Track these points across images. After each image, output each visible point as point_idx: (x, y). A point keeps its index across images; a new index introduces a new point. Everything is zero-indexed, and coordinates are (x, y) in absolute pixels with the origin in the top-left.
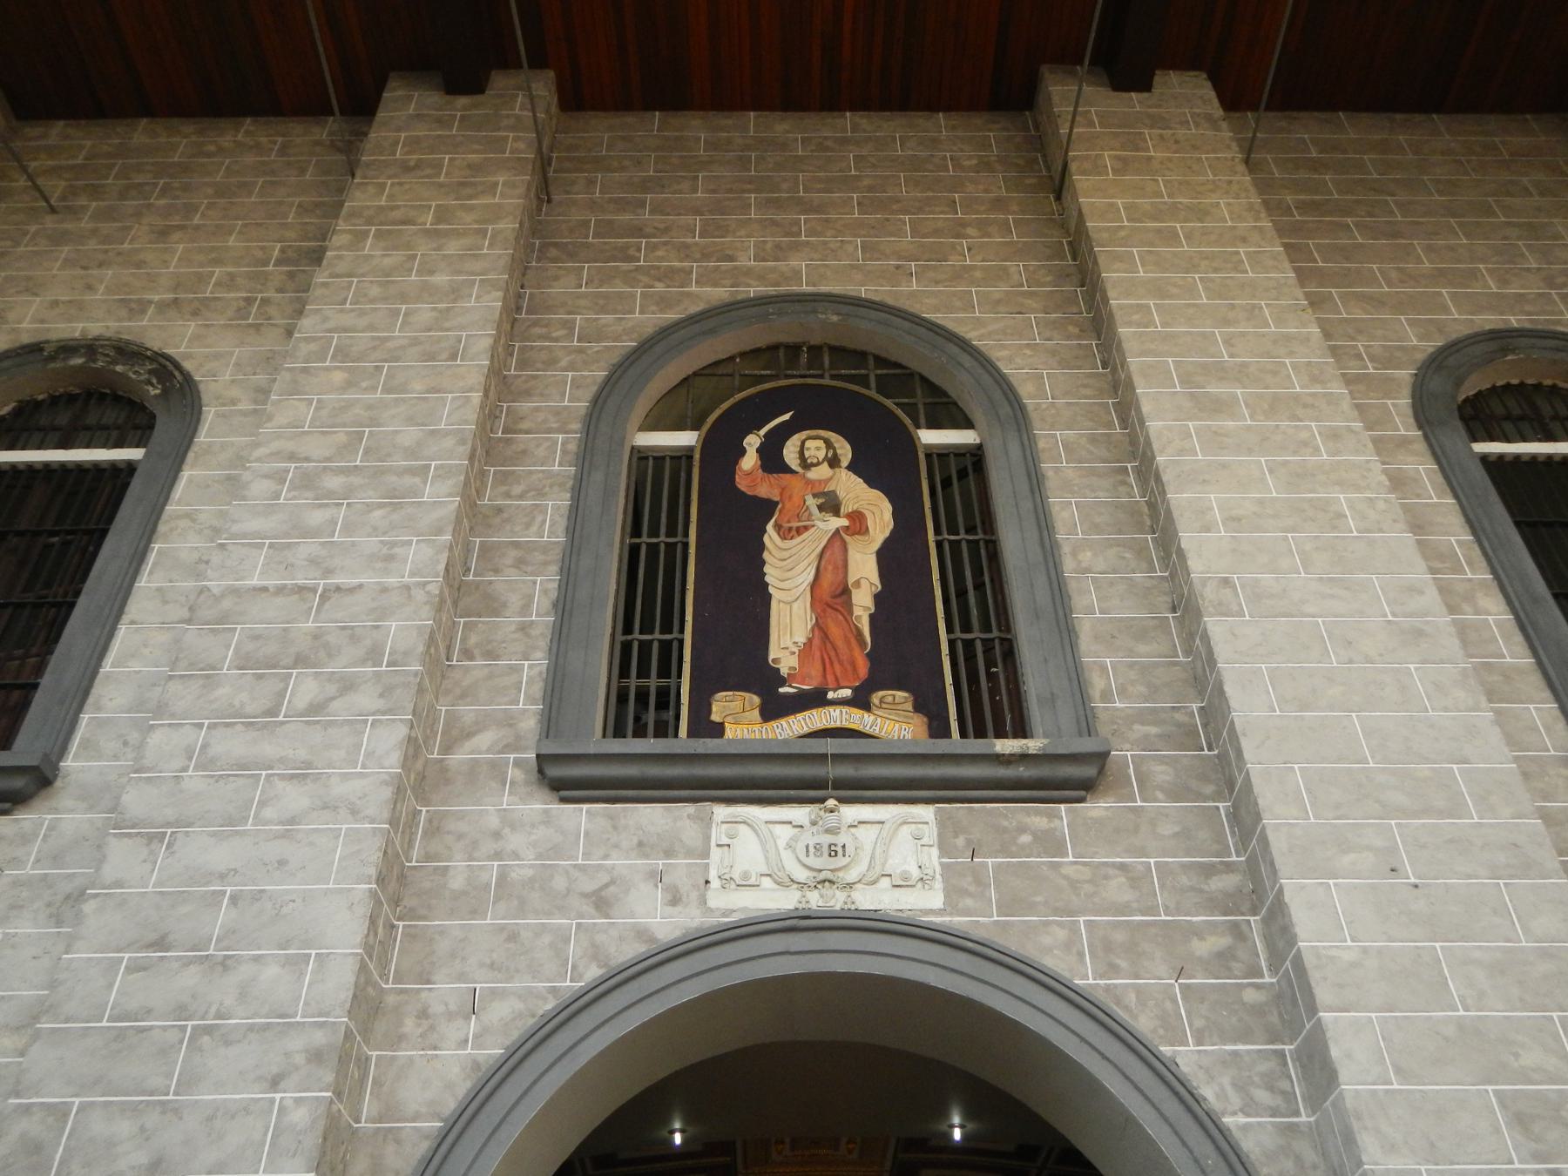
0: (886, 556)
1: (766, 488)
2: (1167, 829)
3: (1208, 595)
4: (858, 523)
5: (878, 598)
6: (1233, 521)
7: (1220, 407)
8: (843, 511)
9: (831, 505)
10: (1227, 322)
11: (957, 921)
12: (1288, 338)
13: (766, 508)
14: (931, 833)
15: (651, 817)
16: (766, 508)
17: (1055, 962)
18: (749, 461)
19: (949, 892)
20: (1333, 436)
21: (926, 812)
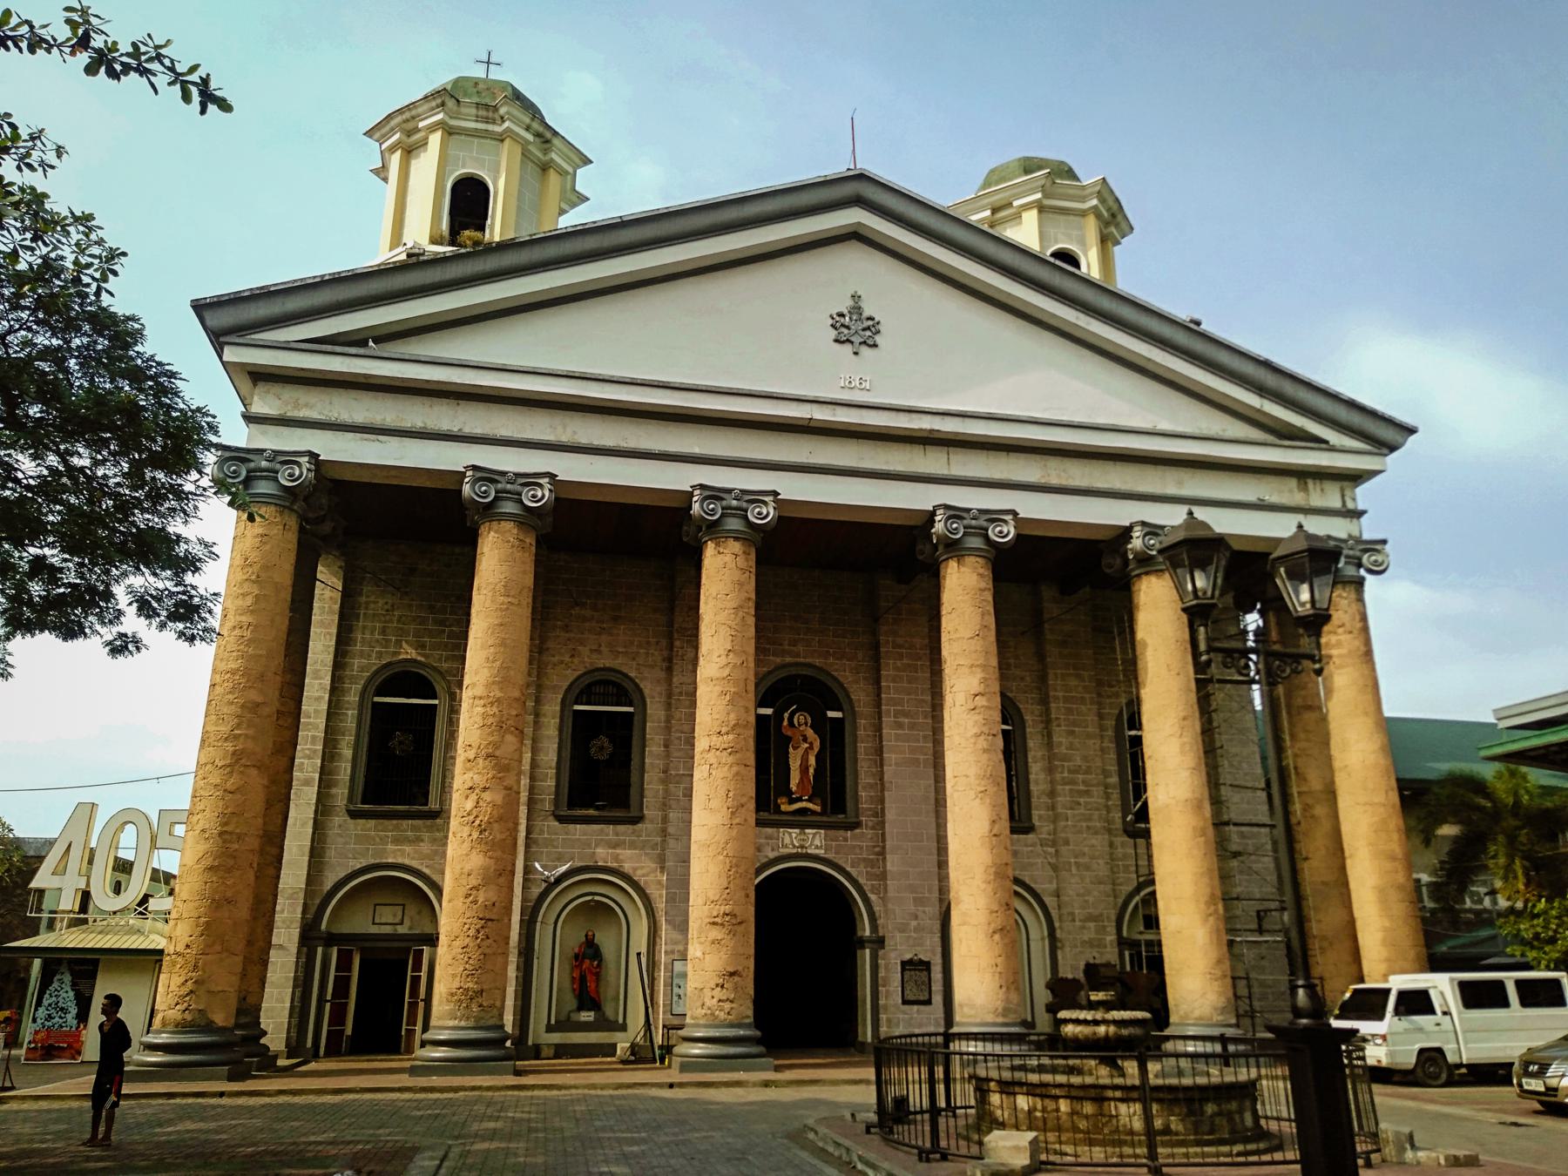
0: (818, 757)
1: (789, 733)
2: (869, 836)
3: (887, 785)
4: (811, 747)
5: (815, 770)
6: (896, 764)
7: (900, 726)
8: (809, 740)
9: (805, 740)
10: (909, 694)
11: (826, 856)
12: (923, 700)
13: (789, 739)
14: (823, 836)
15: (769, 830)
16: (789, 739)
17: (844, 865)
18: (785, 723)
19: (826, 850)
20: (925, 737)
21: (822, 831)
